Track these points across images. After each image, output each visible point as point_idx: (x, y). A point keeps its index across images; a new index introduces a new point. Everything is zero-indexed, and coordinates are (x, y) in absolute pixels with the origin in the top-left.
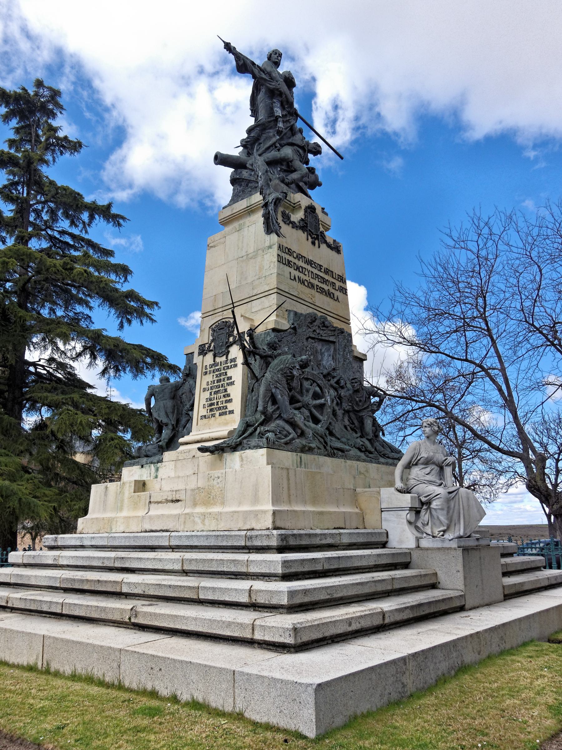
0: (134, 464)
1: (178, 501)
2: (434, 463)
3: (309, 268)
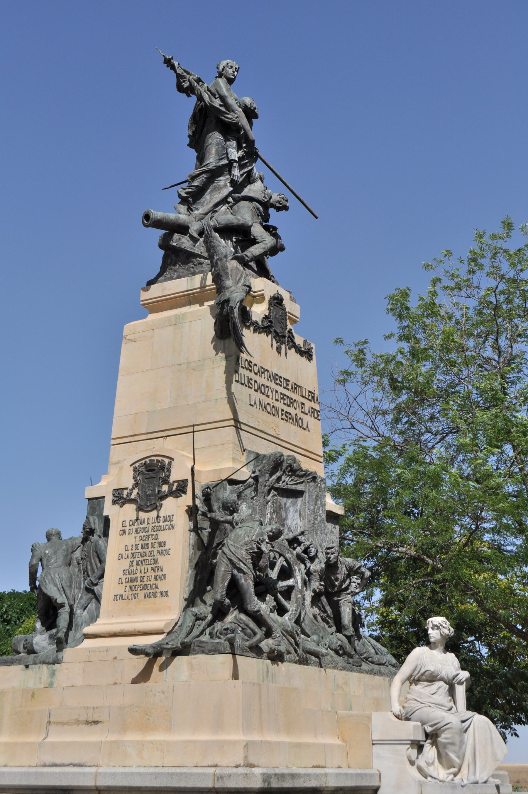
0: (11, 663)
1: (96, 722)
2: (442, 679)
3: (273, 385)
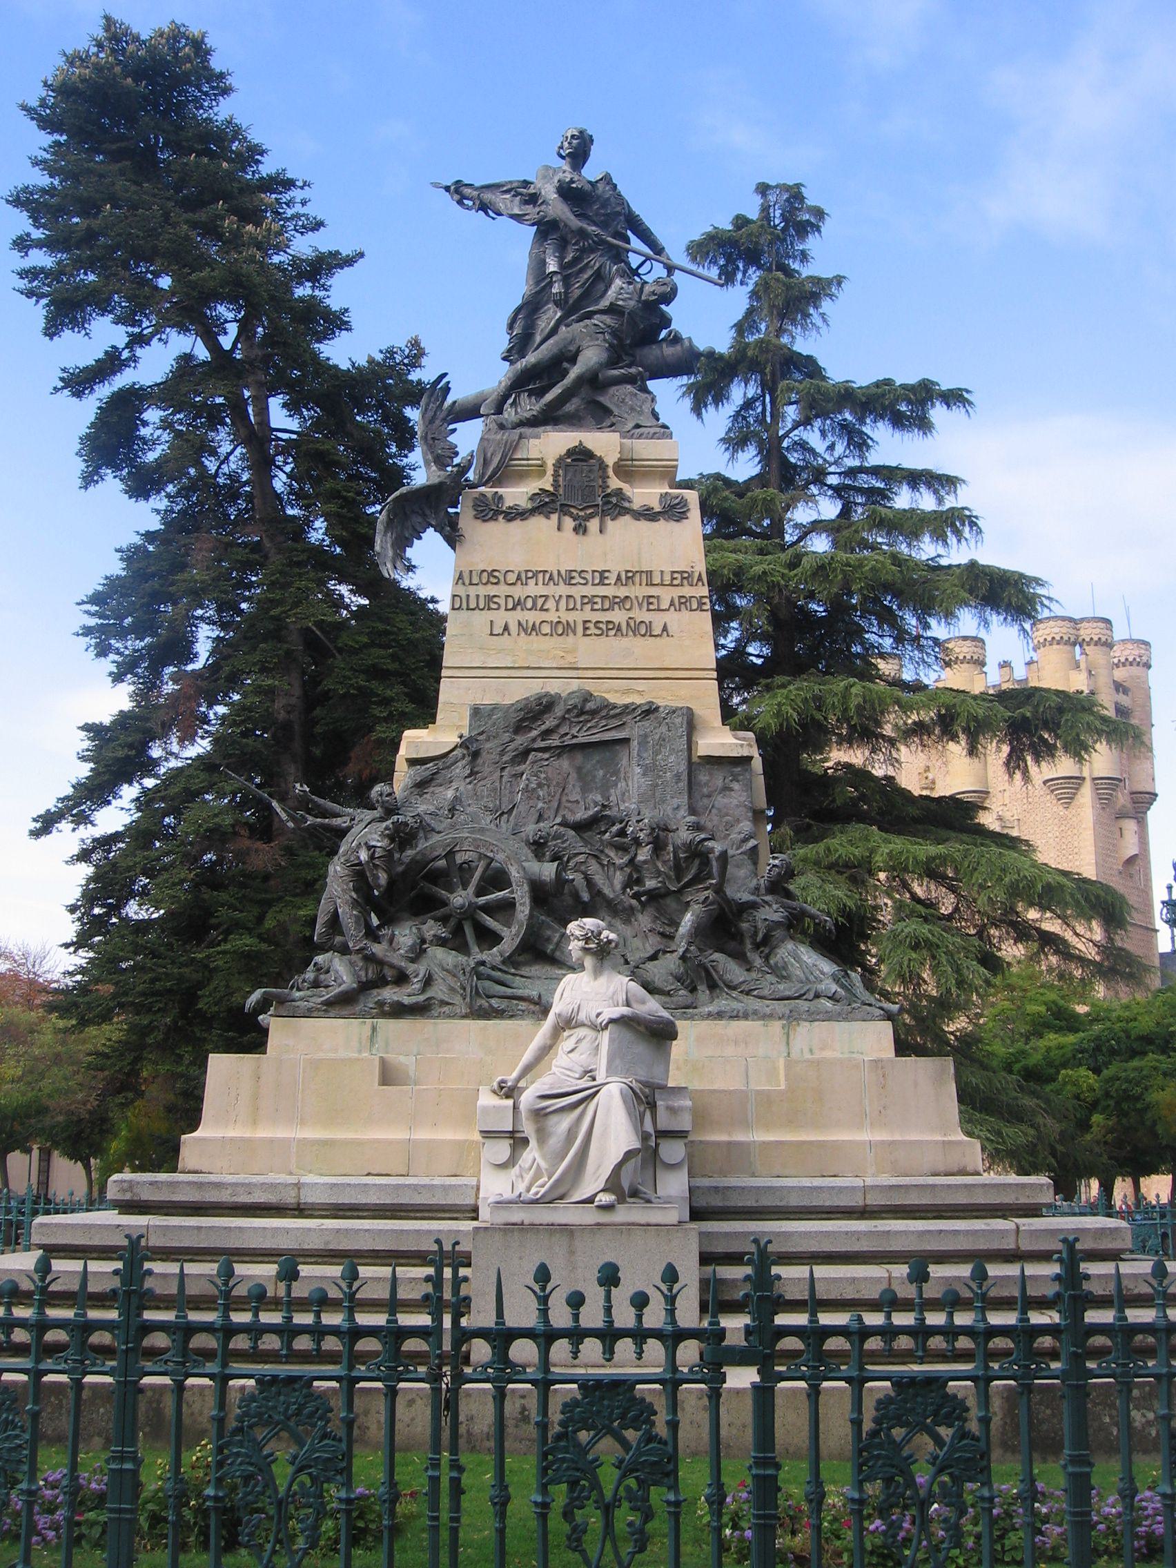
2: (583, 1025)
3: (563, 590)
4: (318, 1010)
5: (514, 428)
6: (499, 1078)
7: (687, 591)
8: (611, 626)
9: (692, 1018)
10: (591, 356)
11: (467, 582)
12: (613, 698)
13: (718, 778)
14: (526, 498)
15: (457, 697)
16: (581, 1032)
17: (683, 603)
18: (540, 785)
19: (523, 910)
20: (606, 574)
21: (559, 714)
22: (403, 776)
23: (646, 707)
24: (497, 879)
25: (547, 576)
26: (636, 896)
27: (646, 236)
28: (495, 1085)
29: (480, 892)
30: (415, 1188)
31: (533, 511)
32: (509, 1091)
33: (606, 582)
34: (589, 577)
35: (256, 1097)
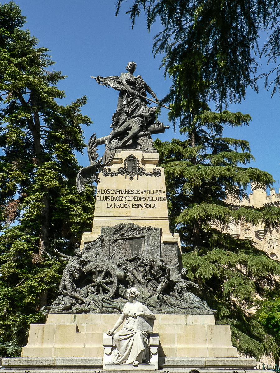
3: (127, 195)
4: (60, 311)
5: (114, 149)
6: (109, 331)
7: (160, 195)
8: (140, 205)
9: (160, 313)
10: (135, 128)
11: (101, 193)
12: (140, 225)
13: (169, 247)
14: (117, 169)
15: (98, 225)
16: (130, 318)
17: (159, 199)
18: (120, 249)
19: (116, 282)
20: (138, 191)
21: (126, 229)
22: (82, 246)
23: (149, 228)
24: (108, 274)
25: (123, 191)
26: (146, 280)
27: (150, 92)
28: (108, 333)
29: (104, 278)
30: (86, 360)
31: (119, 173)
32: (111, 334)
33: (138, 193)
34: (134, 191)
35: (43, 336)
